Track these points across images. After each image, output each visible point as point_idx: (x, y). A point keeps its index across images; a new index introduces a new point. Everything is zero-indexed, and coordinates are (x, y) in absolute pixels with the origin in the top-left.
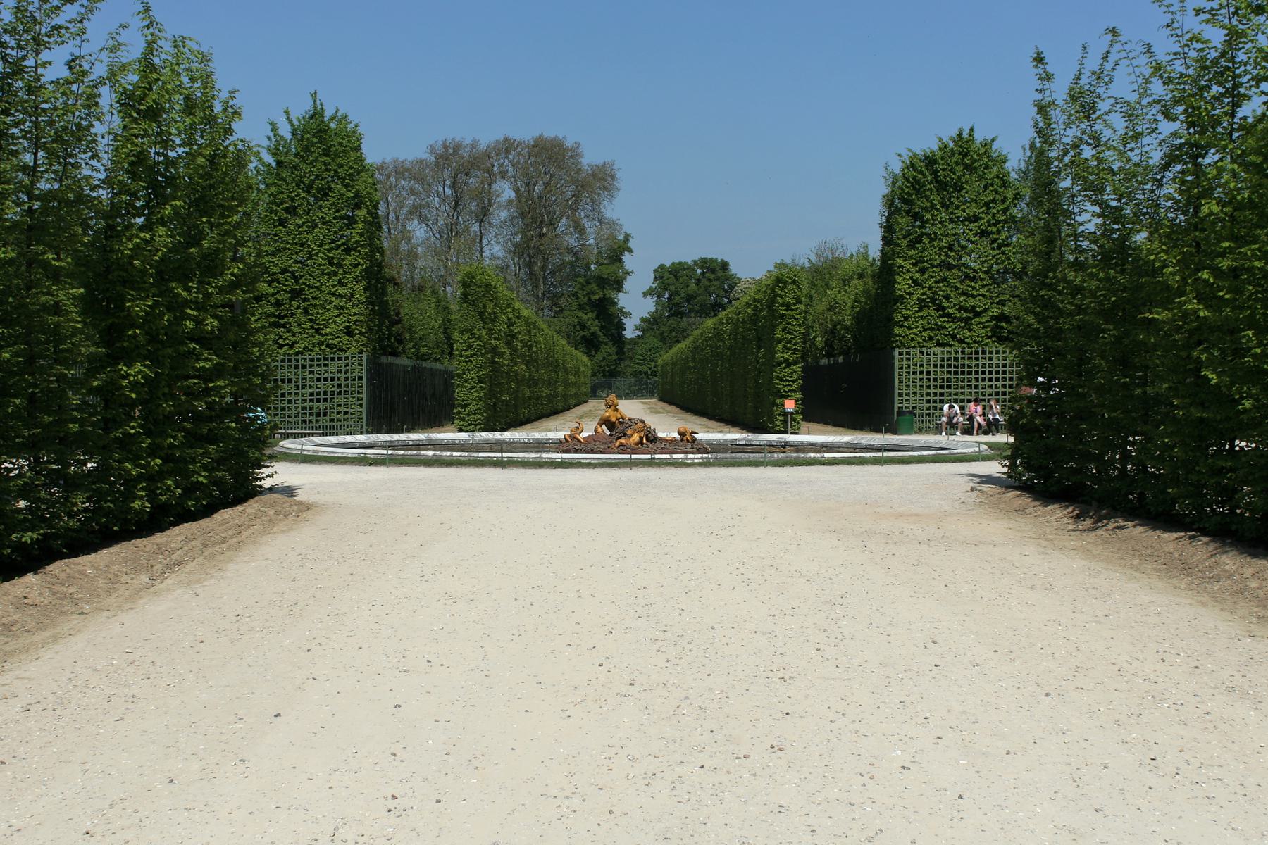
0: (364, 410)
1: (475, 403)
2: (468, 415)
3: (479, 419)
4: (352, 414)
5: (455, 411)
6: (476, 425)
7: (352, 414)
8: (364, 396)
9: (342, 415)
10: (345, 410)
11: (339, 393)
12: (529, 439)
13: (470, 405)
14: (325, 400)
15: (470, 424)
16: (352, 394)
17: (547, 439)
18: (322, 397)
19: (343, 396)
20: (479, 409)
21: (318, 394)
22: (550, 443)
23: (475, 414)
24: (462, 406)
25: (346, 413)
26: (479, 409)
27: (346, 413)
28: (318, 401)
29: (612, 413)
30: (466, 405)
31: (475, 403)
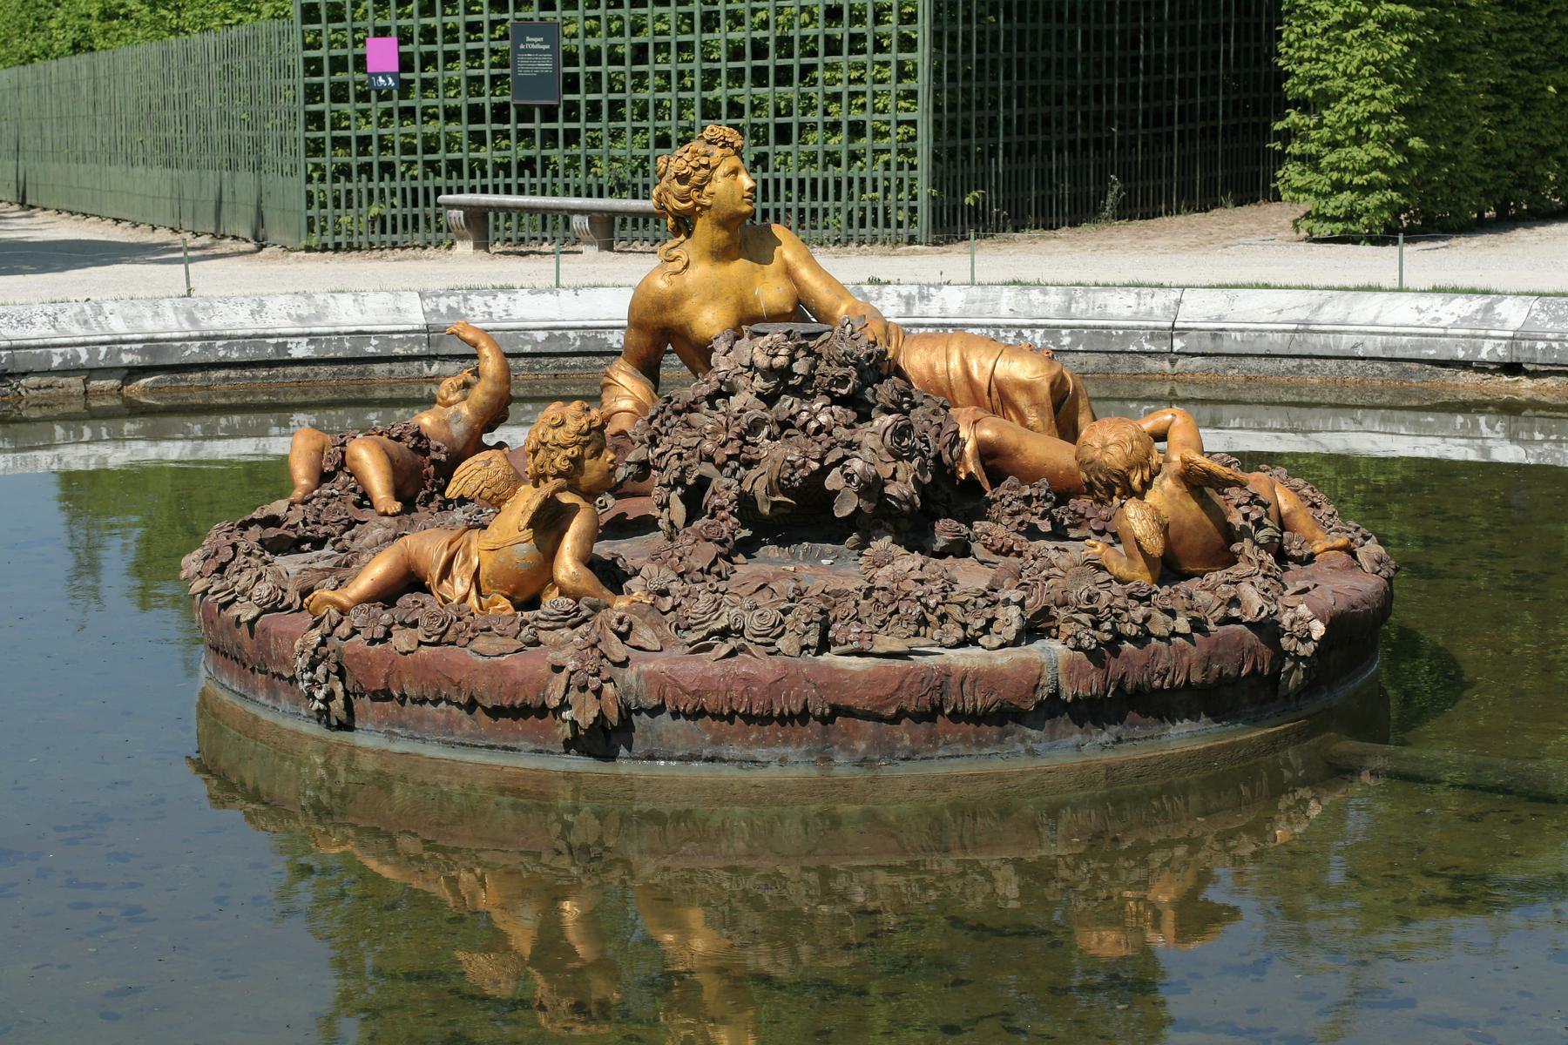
0: (922, 113)
1: (1359, 89)
2: (1334, 145)
3: (1376, 163)
4: (878, 134)
5: (1278, 126)
6: (1367, 189)
7: (878, 134)
8: (921, 57)
9: (843, 135)
10: (857, 115)
11: (833, 47)
12: (1052, 331)
13: (1338, 97)
14: (784, 76)
15: (1339, 187)
16: (879, 47)
17: (1156, 334)
18: (771, 61)
19: (844, 59)
20: (1374, 116)
21: (759, 50)
22: (1173, 356)
23: (1358, 140)
24: (1304, 106)
25: (857, 130)
26: (1385, 119)
27: (857, 130)
28: (760, 77)
29: (702, 272)
30: (1327, 99)
31: (1359, 89)
